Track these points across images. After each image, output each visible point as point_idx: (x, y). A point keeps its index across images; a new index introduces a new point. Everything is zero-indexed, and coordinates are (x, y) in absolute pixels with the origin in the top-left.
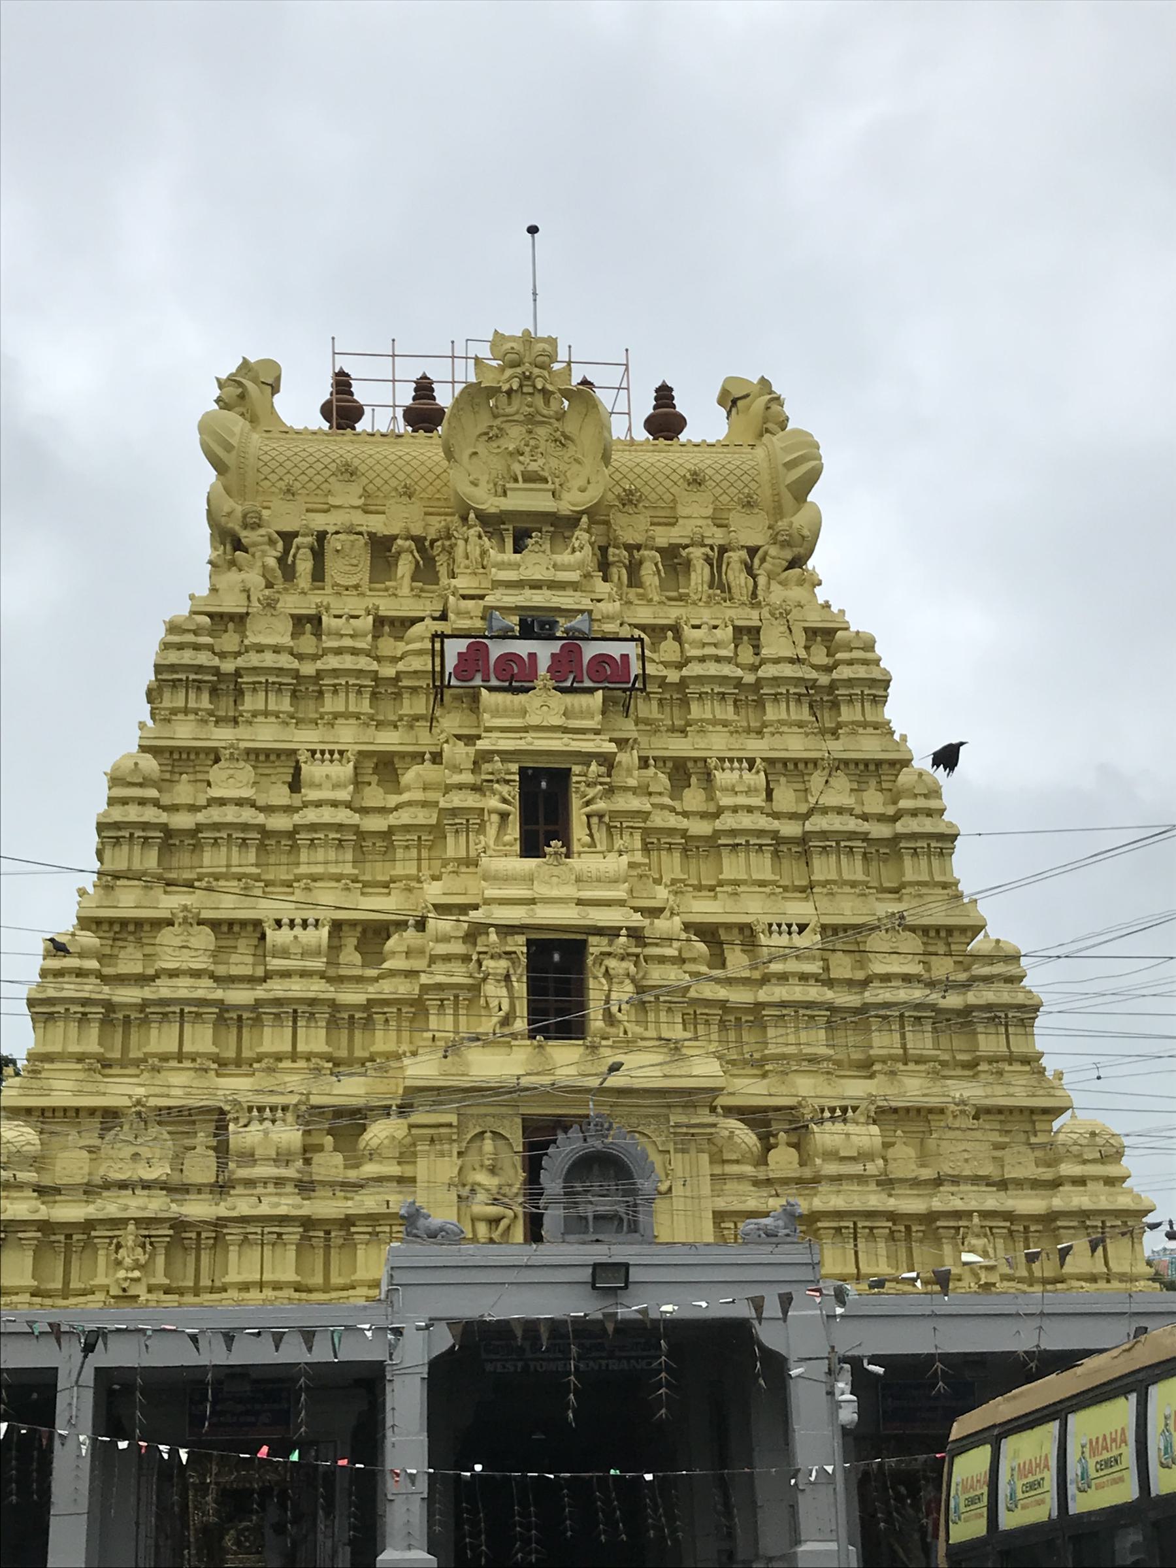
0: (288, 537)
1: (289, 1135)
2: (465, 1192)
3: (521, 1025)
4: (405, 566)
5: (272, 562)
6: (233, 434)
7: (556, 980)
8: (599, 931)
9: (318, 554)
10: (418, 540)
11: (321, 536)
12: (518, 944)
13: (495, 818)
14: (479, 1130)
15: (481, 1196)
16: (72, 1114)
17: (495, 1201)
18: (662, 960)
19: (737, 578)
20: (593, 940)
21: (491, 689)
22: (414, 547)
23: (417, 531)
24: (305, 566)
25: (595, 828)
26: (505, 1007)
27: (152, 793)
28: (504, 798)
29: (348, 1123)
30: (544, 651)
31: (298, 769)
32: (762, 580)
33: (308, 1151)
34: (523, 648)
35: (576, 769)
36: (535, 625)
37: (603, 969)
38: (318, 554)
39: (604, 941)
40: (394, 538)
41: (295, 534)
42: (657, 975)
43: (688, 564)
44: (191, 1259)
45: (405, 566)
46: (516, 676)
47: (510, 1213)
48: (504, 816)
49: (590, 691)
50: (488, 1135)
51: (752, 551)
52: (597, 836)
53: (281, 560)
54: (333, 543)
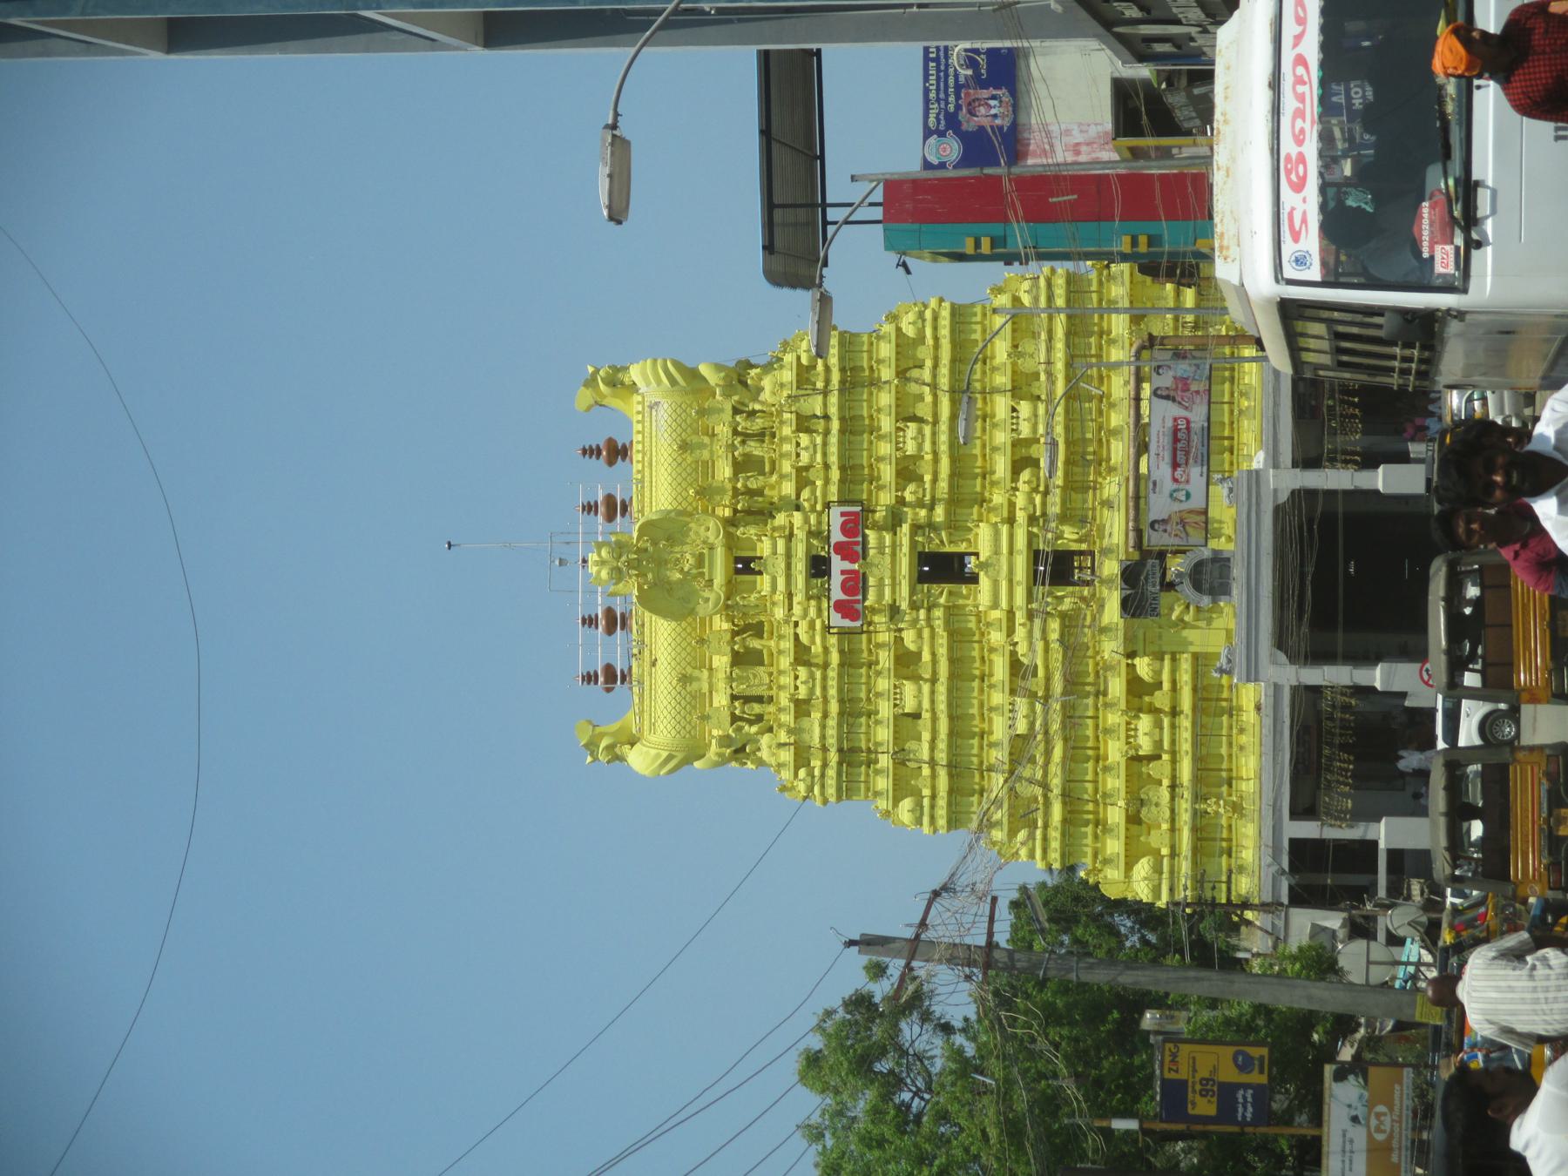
0: (734, 719)
1: (1144, 723)
4: (755, 644)
5: (754, 729)
6: (658, 755)
7: (1058, 568)
9: (748, 699)
10: (735, 634)
11: (734, 698)
16: (1129, 841)
17: (1188, 607)
18: (1044, 504)
21: (865, 598)
23: (728, 636)
24: (757, 708)
27: (926, 802)
28: (942, 593)
29: (1137, 688)
30: (838, 564)
31: (908, 715)
32: (757, 407)
33: (1154, 711)
34: (837, 579)
36: (818, 567)
38: (748, 699)
41: (733, 715)
42: (1055, 509)
43: (746, 455)
45: (755, 644)
46: (856, 584)
48: (950, 593)
49: (865, 537)
53: (751, 723)
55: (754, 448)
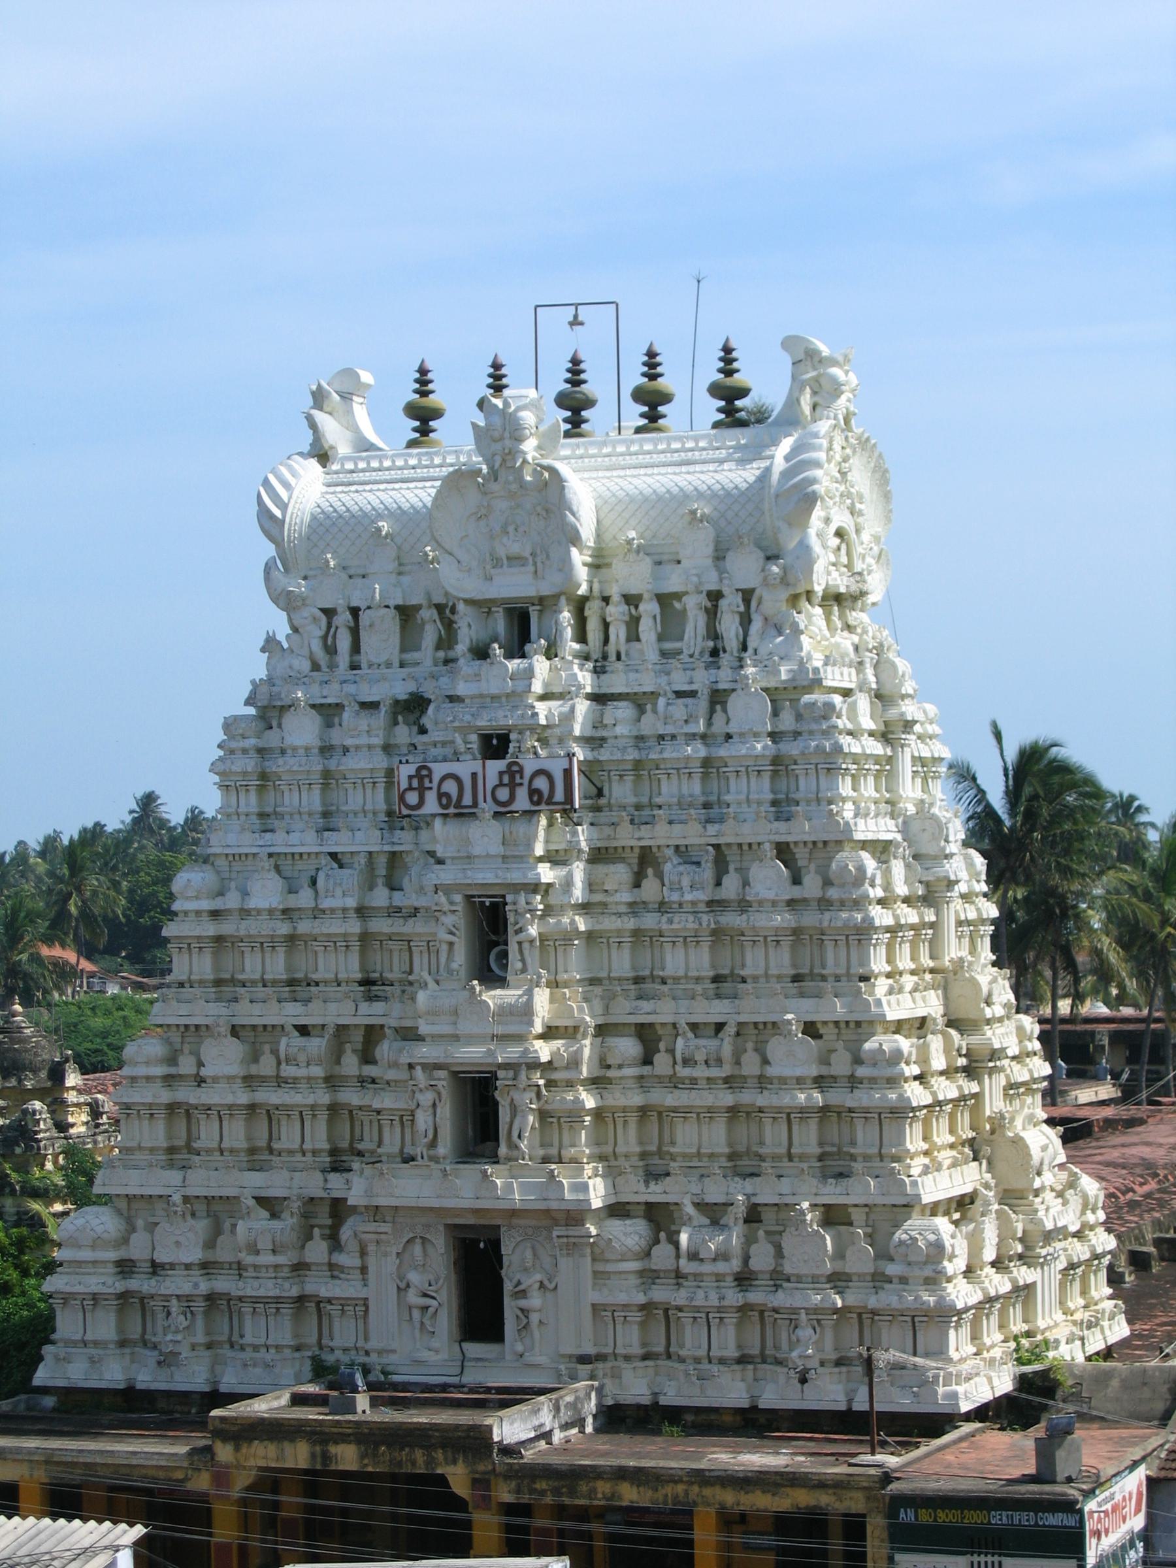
0: (329, 613)
2: (403, 1285)
3: (445, 1148)
4: (430, 636)
5: (317, 647)
8: (506, 1066)
9: (355, 632)
12: (442, 1080)
13: (445, 947)
14: (411, 1235)
15: (412, 1292)
19: (729, 626)
20: (501, 1074)
22: (436, 617)
25: (526, 953)
26: (430, 1135)
35: (509, 898)
37: (509, 1100)
38: (355, 632)
39: (511, 1074)
40: (418, 608)
44: (226, 1319)
47: (434, 1303)
50: (418, 1241)
51: (747, 595)
52: (529, 960)
54: (364, 618)
55: (696, 622)
